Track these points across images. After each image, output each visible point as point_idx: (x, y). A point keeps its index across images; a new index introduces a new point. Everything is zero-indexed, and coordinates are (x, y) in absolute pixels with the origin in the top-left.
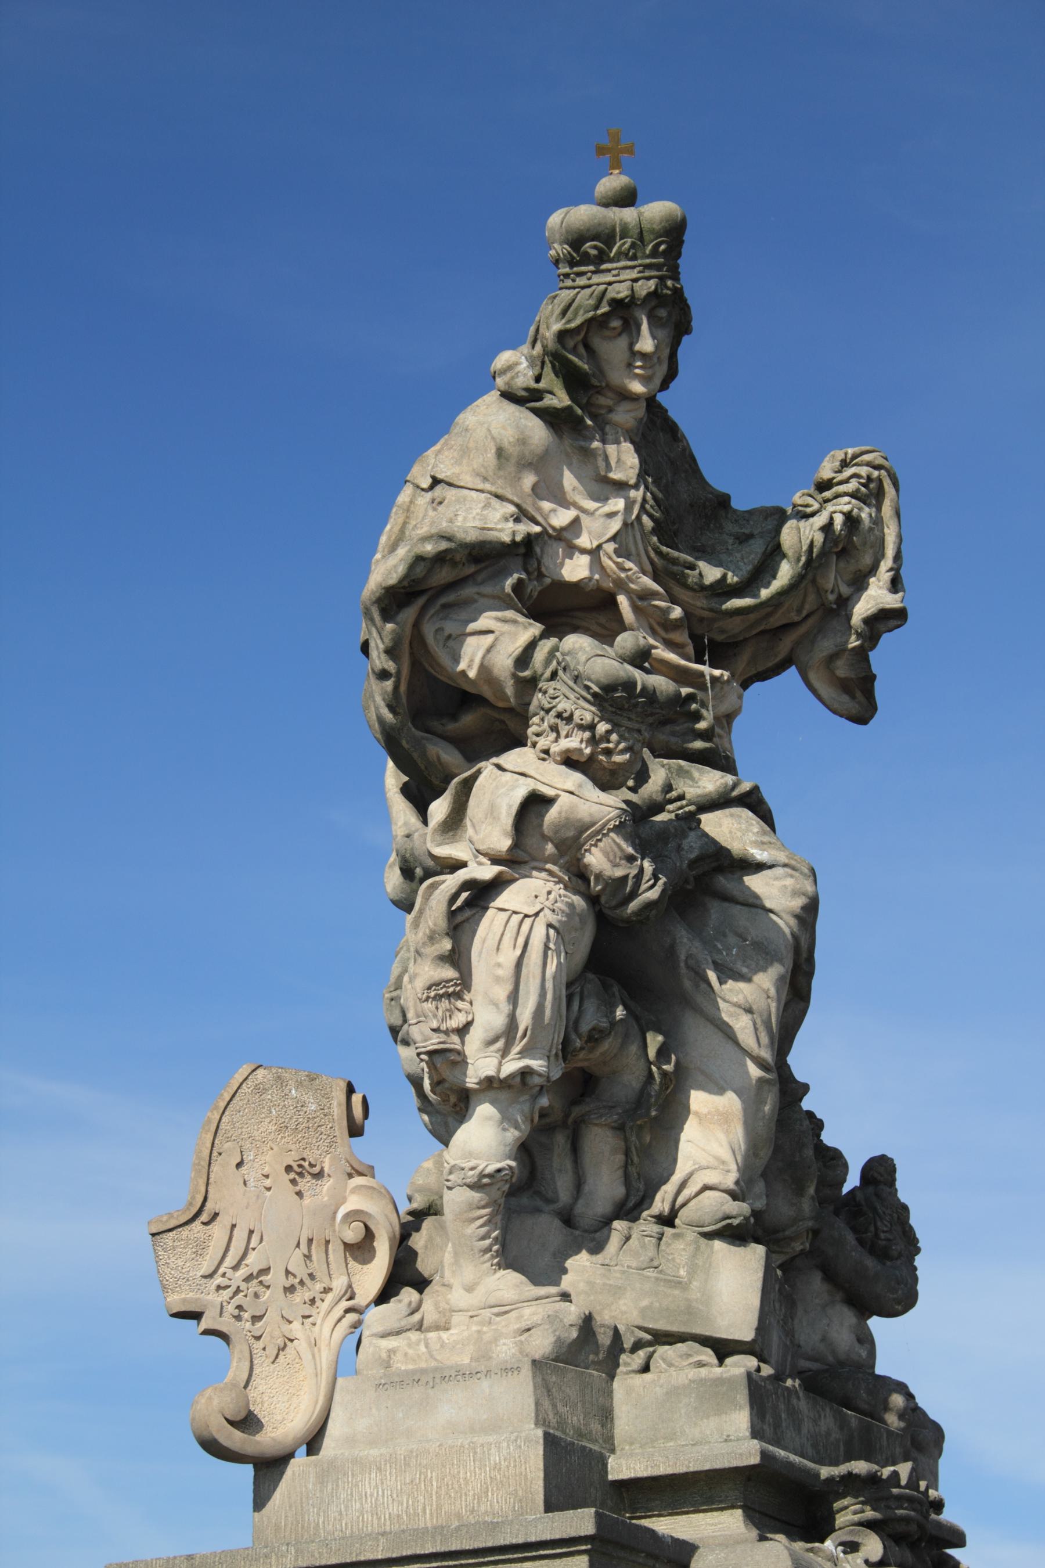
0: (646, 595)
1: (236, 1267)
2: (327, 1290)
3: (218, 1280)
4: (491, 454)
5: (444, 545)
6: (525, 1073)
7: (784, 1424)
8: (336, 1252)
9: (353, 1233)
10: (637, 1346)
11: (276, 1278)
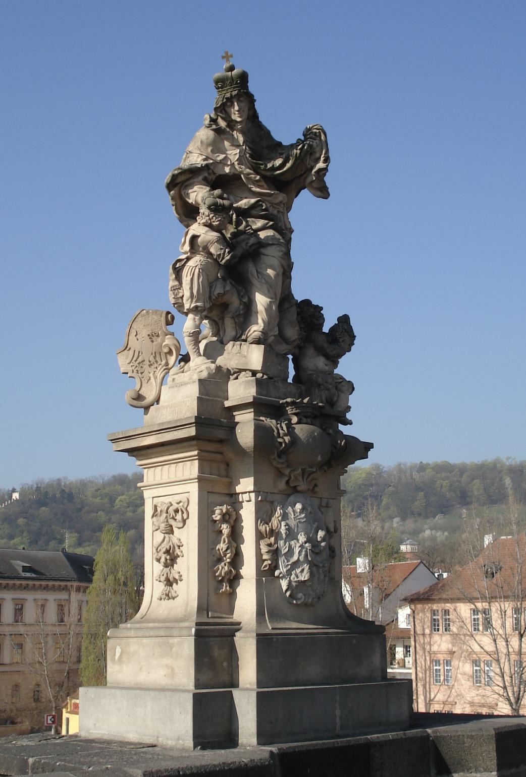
0: (249, 174)
1: (136, 361)
2: (160, 364)
3: (132, 364)
4: (200, 143)
5: (180, 171)
6: (196, 307)
9: (166, 350)
10: (235, 373)
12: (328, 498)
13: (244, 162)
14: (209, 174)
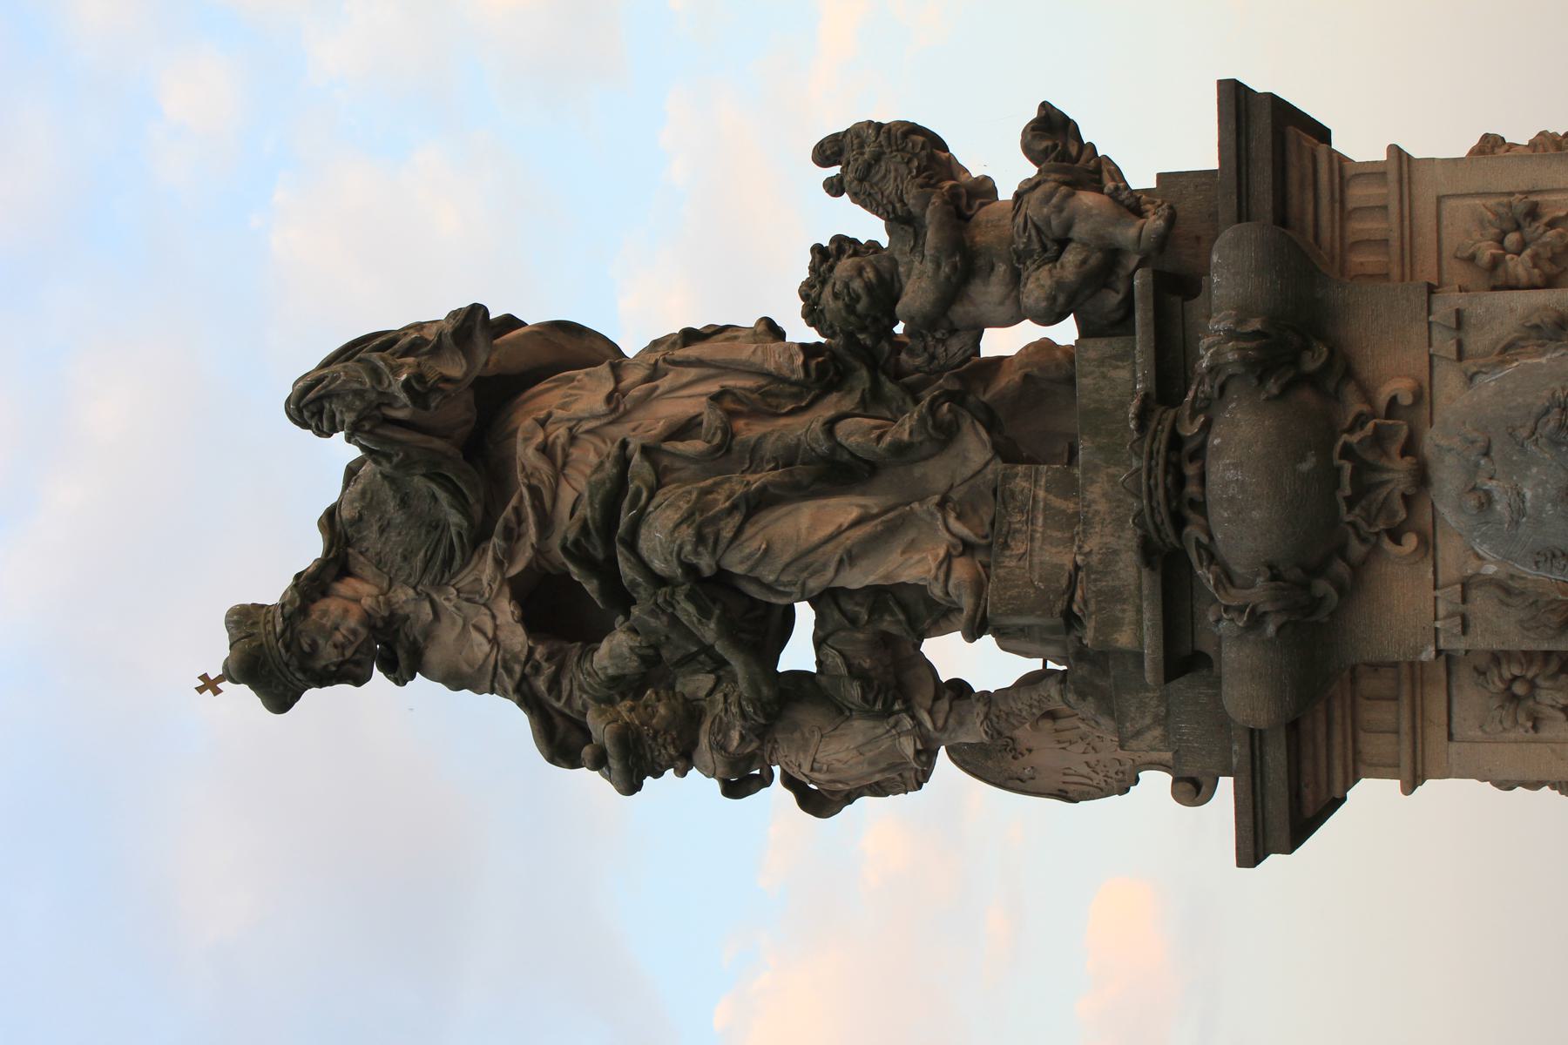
0: (499, 563)
7: (1117, 583)
8: (1062, 724)
9: (1047, 725)
12: (1430, 324)
13: (471, 578)
14: (537, 669)
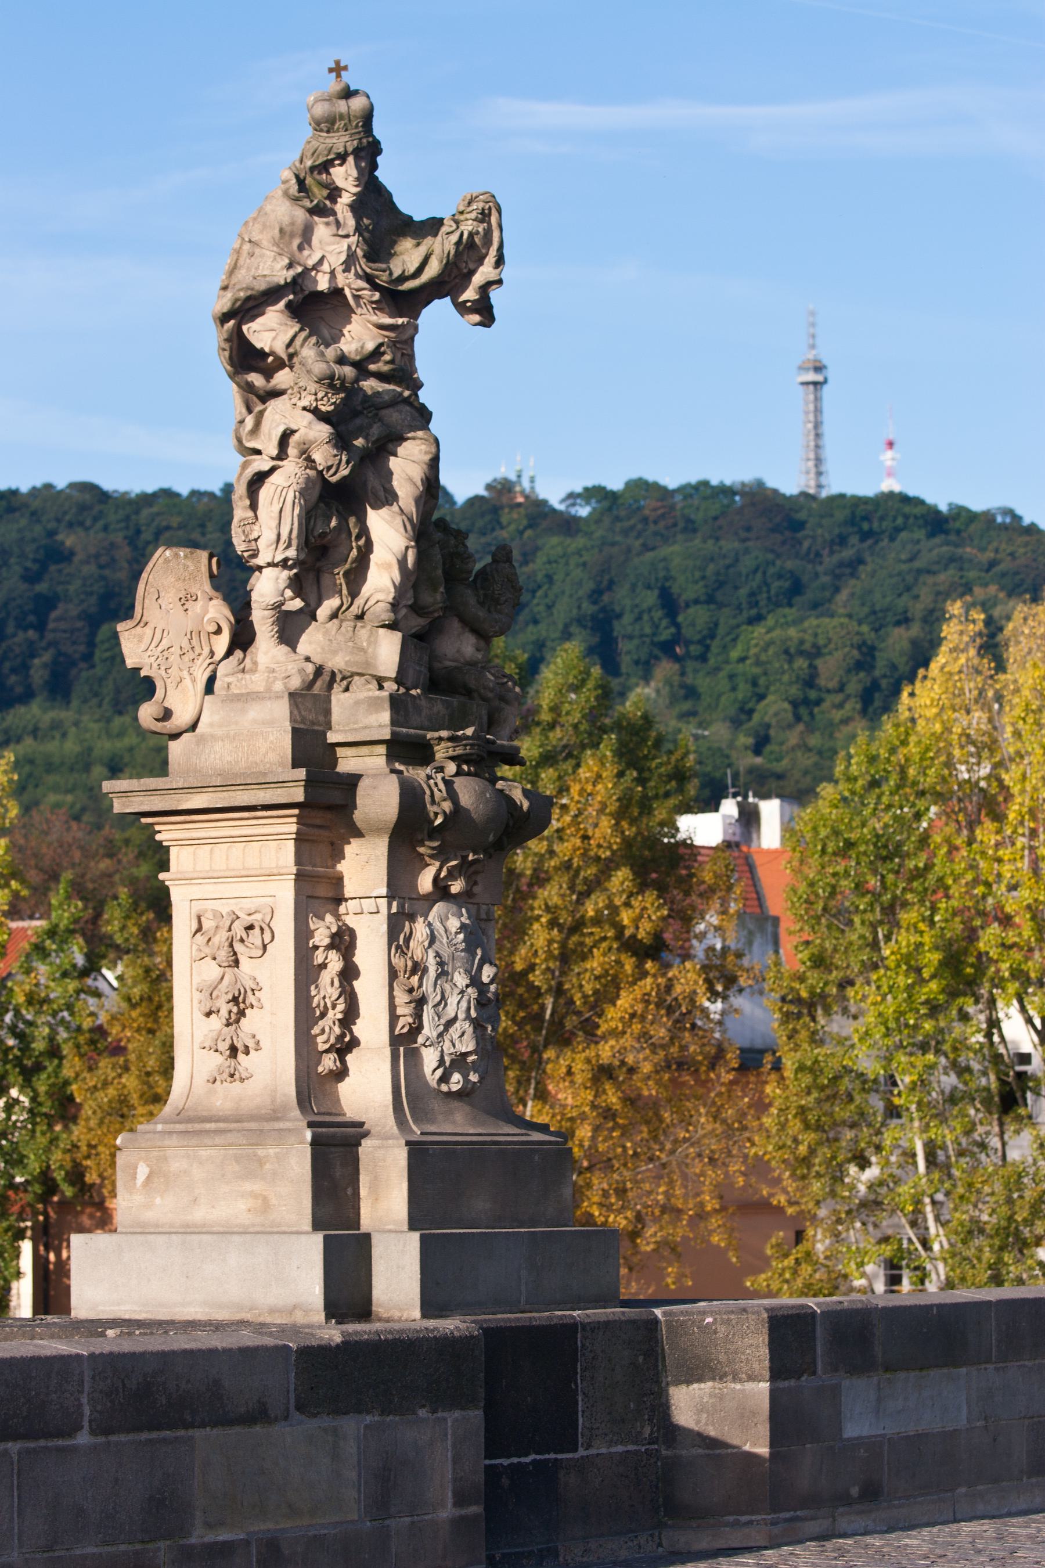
3: (149, 653)
4: (277, 231)
5: (249, 293)
6: (286, 560)
9: (213, 628)
10: (343, 678)
11: (176, 650)
